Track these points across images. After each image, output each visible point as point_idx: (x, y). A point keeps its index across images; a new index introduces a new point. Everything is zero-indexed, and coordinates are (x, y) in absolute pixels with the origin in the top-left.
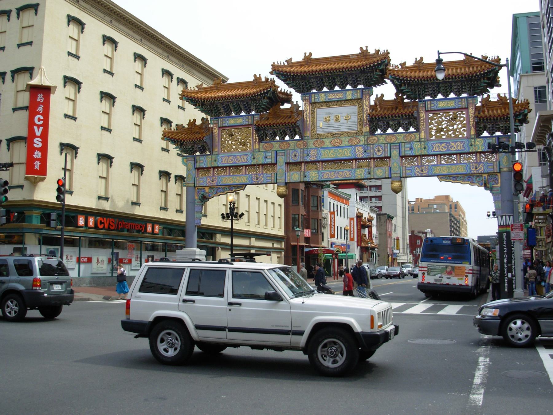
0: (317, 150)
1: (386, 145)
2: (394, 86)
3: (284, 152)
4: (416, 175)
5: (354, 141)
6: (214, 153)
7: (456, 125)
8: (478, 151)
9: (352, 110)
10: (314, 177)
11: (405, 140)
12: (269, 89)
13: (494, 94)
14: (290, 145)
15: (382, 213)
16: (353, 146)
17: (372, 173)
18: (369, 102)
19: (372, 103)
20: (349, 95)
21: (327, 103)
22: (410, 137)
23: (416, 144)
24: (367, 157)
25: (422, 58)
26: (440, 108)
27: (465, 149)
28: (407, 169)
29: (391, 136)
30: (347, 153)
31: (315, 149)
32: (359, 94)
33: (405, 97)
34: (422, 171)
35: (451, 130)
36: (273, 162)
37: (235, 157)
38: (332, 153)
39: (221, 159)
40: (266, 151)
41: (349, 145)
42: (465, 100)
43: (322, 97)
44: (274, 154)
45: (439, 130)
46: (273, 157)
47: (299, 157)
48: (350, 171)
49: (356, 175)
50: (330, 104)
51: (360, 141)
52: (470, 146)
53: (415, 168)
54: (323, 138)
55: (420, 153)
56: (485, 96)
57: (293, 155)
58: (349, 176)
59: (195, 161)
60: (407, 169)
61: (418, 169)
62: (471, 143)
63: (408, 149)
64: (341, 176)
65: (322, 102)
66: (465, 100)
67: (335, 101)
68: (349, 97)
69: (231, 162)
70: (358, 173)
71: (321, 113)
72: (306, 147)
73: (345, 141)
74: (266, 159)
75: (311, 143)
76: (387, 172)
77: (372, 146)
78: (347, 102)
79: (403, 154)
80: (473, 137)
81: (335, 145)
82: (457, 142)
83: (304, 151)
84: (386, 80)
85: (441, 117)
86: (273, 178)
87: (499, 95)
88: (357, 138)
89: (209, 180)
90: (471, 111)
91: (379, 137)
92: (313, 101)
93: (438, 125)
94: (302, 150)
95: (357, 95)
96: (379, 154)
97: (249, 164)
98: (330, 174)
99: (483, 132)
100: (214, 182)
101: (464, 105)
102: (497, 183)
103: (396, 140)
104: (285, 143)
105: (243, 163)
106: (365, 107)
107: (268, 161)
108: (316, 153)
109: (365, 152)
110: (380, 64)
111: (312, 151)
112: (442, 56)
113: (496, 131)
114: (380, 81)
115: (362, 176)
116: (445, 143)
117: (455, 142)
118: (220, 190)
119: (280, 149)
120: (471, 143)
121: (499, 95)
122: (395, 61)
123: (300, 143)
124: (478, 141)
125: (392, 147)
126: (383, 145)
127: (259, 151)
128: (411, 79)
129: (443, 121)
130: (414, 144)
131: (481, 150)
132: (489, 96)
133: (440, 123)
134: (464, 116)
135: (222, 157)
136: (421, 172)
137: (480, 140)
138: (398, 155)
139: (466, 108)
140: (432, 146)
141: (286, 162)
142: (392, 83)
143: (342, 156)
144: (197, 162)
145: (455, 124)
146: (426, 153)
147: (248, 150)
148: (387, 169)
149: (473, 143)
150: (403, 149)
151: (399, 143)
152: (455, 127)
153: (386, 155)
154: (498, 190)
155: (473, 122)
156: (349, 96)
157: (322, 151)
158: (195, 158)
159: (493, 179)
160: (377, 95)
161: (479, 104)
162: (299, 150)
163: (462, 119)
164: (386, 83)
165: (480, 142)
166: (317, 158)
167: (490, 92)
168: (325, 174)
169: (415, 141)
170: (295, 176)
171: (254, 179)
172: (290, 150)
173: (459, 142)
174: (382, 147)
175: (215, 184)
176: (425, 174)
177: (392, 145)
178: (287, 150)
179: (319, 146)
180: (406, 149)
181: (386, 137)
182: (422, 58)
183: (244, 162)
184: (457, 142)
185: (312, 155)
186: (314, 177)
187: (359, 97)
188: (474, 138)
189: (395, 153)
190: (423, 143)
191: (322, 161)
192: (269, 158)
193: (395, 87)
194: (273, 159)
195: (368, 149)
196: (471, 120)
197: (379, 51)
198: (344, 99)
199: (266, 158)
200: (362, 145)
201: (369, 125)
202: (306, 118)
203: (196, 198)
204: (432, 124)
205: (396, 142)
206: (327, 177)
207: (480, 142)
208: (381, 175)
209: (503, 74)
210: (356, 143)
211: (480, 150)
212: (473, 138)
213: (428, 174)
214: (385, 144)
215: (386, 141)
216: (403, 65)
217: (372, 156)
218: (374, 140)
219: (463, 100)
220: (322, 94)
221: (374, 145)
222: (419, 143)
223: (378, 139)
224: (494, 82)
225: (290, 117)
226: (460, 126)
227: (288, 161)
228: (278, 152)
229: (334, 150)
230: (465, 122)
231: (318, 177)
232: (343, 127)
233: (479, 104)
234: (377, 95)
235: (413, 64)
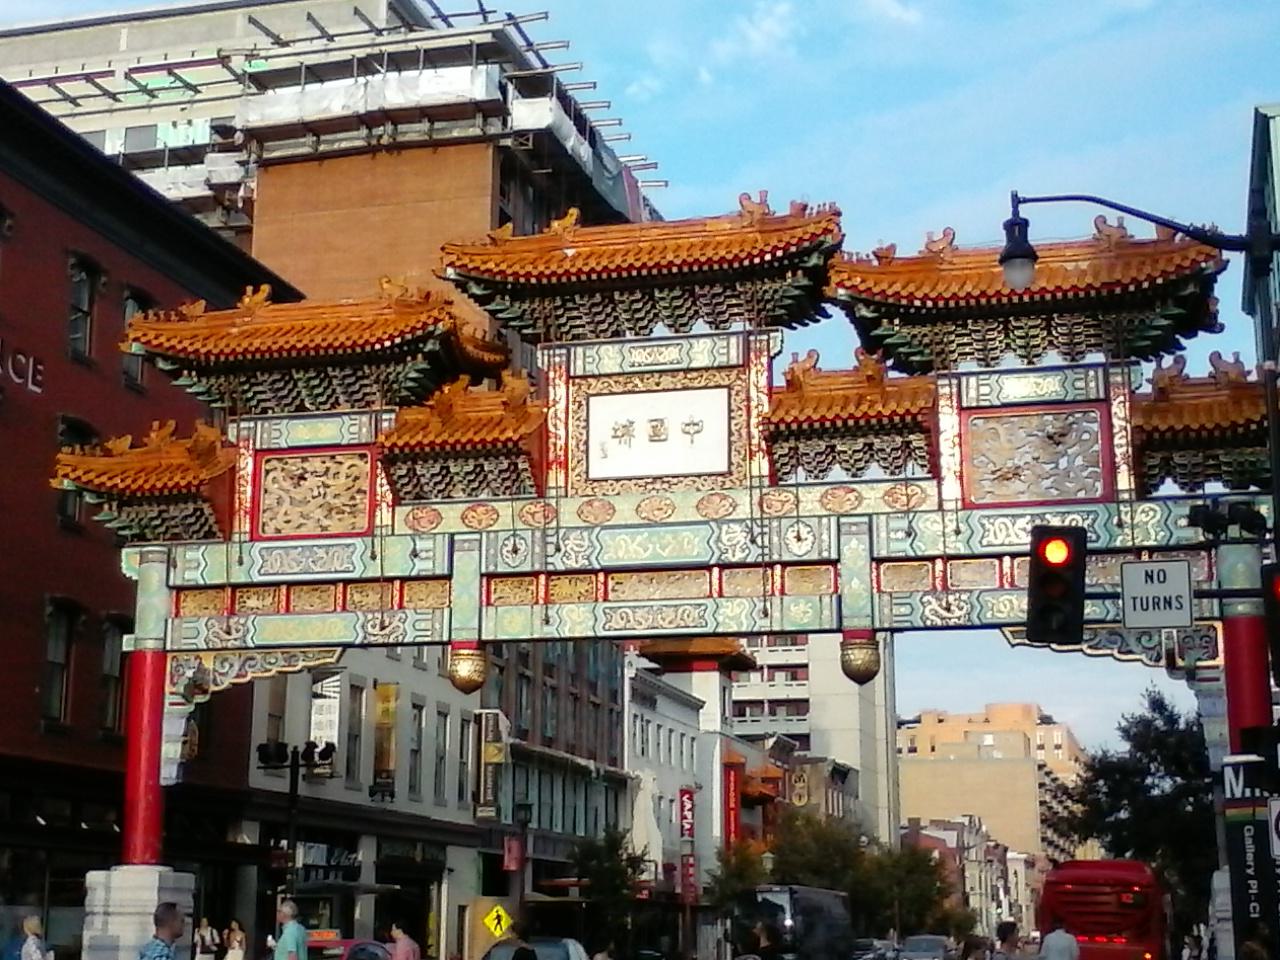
0: (589, 535)
1: (825, 520)
2: (852, 327)
3: (477, 536)
4: (929, 623)
5: (715, 506)
6: (236, 537)
7: (1066, 458)
8: (1146, 543)
9: (710, 406)
10: (580, 623)
11: (890, 506)
12: (431, 328)
13: (1198, 355)
15: (809, 754)
16: (712, 524)
17: (777, 614)
18: (770, 378)
20: (702, 352)
22: (907, 495)
23: (927, 520)
24: (760, 559)
26: (1011, 399)
27: (1098, 537)
28: (894, 601)
29: (841, 493)
30: (692, 546)
31: (587, 528)
32: (733, 352)
33: (890, 363)
34: (948, 609)
36: (438, 572)
37: (308, 553)
38: (639, 545)
39: (262, 557)
40: (416, 534)
41: (700, 518)
42: (1096, 373)
43: (609, 358)
44: (442, 544)
47: (529, 557)
48: (700, 605)
49: (720, 619)
50: (637, 381)
52: (1116, 529)
53: (925, 599)
54: (610, 493)
55: (942, 548)
56: (1168, 361)
57: (510, 548)
58: (698, 621)
59: (171, 563)
60: (894, 601)
61: (933, 601)
62: (1120, 520)
63: (901, 535)
64: (670, 622)
65: (609, 376)
66: (1096, 373)
67: (652, 372)
69: (296, 570)
70: (728, 611)
71: (606, 411)
72: (554, 524)
73: (685, 503)
74: (416, 560)
76: (826, 612)
77: (775, 524)
78: (695, 374)
79: (884, 553)
80: (1126, 496)
81: (652, 517)
82: (1069, 513)
83: (545, 535)
84: (829, 308)
86: (437, 626)
87: (1215, 358)
88: (725, 497)
89: (216, 629)
90: (1119, 410)
91: (800, 495)
92: (580, 372)
94: (538, 534)
95: (728, 352)
96: (799, 550)
98: (634, 612)
99: (1163, 482)
100: (235, 635)
101: (1093, 387)
102: (1214, 656)
103: (860, 504)
104: (481, 509)
105: (336, 572)
106: (753, 393)
107: (423, 567)
108: (586, 543)
109: (753, 541)
110: (808, 252)
111: (574, 535)
112: (1025, 211)
113: (1208, 478)
114: (806, 309)
115: (742, 624)
116: (1028, 518)
117: (1064, 513)
118: (252, 663)
119: (466, 530)
120: (1120, 520)
121: (1215, 358)
122: (858, 243)
123: (533, 509)
124: (1143, 511)
125: (844, 529)
126: (816, 520)
127: (393, 534)
128: (912, 302)
130: (920, 517)
131: (1156, 540)
132: (1180, 362)
134: (1095, 427)
135: (264, 552)
136: (945, 614)
137: (1152, 509)
138: (867, 553)
139: (1106, 402)
140: (983, 525)
141: (484, 570)
142: (847, 315)
143: (675, 554)
144: (175, 567)
146: (963, 551)
148: (826, 600)
149: (1127, 519)
150: (883, 535)
151: (870, 516)
153: (825, 555)
154: (1217, 680)
155: (1124, 449)
156: (699, 356)
157: (607, 538)
158: (170, 550)
159: (1198, 641)
160: (795, 355)
161: (1147, 389)
162: (530, 532)
163: (1086, 436)
164: (828, 316)
165: (1151, 513)
166: (588, 559)
167: (1183, 348)
168: (616, 617)
169: (924, 507)
170: (514, 621)
171: (374, 627)
172: (497, 531)
173: (1078, 513)
174: (809, 526)
175: (238, 643)
176: (959, 618)
177: (843, 520)
179: (596, 519)
180: (892, 535)
181: (824, 495)
183: (339, 569)
184: (1069, 513)
185: (572, 549)
186: (580, 623)
187: (734, 361)
188: (1130, 502)
189: (854, 551)
190: (949, 516)
192: (427, 558)
193: (856, 328)
194: (439, 561)
195: (762, 534)
196: (1117, 441)
197: (805, 207)
198: (684, 365)
199: (416, 556)
200: (744, 520)
201: (770, 453)
202: (555, 426)
203: (168, 688)
205: (859, 511)
206: (622, 624)
207: (1151, 513)
208: (806, 621)
209: (1229, 288)
210: (722, 512)
211: (1151, 543)
212: (1123, 502)
213: (969, 620)
214: (820, 517)
215: (823, 505)
216: (884, 256)
217: (776, 557)
218: (783, 503)
219: (1092, 373)
220: (609, 347)
221: (784, 521)
222: (937, 517)
224: (1201, 317)
225: (498, 424)
226: (1079, 461)
227: (492, 569)
228: (456, 537)
229: (646, 535)
230: (1097, 447)
231: (591, 623)
233: (1147, 389)
234: (795, 355)
235: (920, 252)
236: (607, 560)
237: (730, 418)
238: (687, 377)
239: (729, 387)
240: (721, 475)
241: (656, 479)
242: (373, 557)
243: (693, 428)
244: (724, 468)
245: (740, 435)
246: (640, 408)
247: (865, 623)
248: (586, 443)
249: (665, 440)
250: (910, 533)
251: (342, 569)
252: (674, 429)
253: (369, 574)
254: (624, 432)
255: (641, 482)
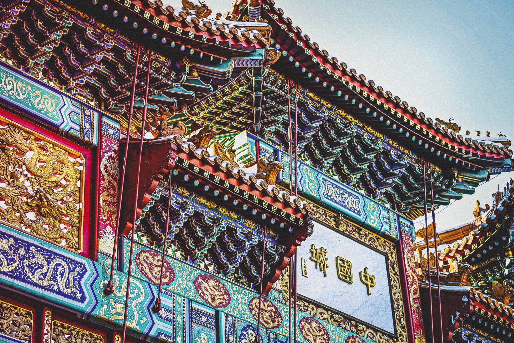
14: (230, 299)
37: (22, 252)
46: (179, 319)
74: (154, 316)
97: (85, 306)
105: (60, 293)
156: (372, 217)
172: (233, 317)
178: (227, 315)
183: (62, 288)
198: (361, 218)
240: (390, 336)
241: (347, 318)
242: (108, 291)
245: (398, 305)
249: (350, 283)
251: (69, 291)
253: (101, 312)
255: (337, 317)
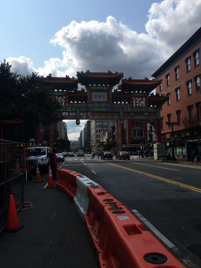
9: (105, 94)
19: (113, 92)
21: (97, 91)
25: (131, 77)
35: (140, 104)
45: (136, 104)
51: (108, 105)
68: (105, 89)
71: (94, 94)
73: (103, 105)
75: (90, 105)
85: (137, 99)
93: (136, 102)
111: (91, 108)
129: (138, 100)
132: (153, 93)
133: (136, 101)
145: (142, 102)
147: (63, 105)
149: (148, 109)
151: (123, 107)
152: (142, 103)
182: (131, 77)
189: (121, 111)
191: (94, 112)
204: (134, 101)
222: (130, 108)
223: (116, 106)
226: (143, 103)
232: (101, 100)
236: (95, 111)
237: (107, 96)
238: (102, 91)
239: (107, 92)
243: (103, 96)
244: (107, 101)
246: (98, 94)
247: (122, 119)
248: (91, 97)
250: (127, 109)
252: (101, 97)
254: (96, 96)
